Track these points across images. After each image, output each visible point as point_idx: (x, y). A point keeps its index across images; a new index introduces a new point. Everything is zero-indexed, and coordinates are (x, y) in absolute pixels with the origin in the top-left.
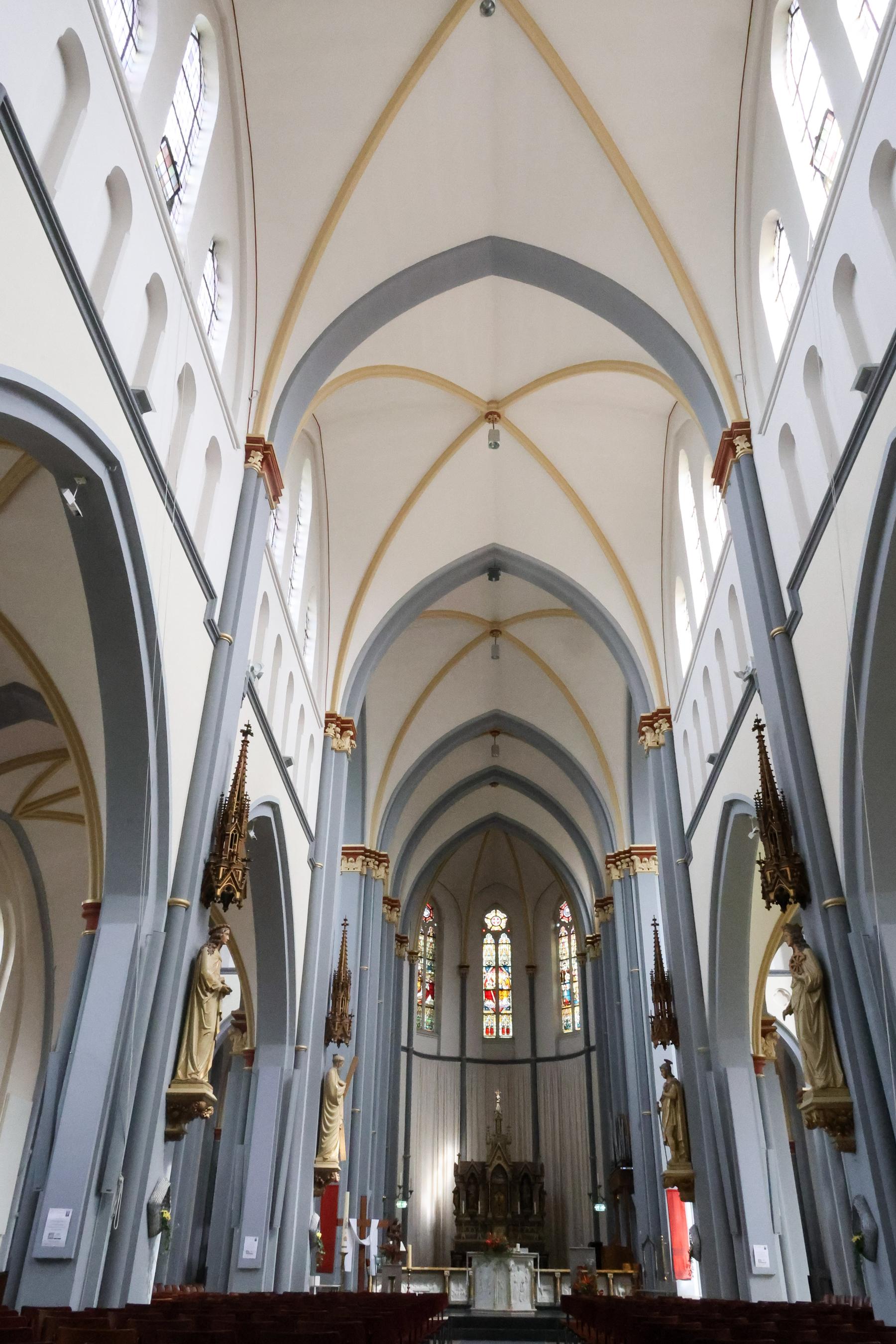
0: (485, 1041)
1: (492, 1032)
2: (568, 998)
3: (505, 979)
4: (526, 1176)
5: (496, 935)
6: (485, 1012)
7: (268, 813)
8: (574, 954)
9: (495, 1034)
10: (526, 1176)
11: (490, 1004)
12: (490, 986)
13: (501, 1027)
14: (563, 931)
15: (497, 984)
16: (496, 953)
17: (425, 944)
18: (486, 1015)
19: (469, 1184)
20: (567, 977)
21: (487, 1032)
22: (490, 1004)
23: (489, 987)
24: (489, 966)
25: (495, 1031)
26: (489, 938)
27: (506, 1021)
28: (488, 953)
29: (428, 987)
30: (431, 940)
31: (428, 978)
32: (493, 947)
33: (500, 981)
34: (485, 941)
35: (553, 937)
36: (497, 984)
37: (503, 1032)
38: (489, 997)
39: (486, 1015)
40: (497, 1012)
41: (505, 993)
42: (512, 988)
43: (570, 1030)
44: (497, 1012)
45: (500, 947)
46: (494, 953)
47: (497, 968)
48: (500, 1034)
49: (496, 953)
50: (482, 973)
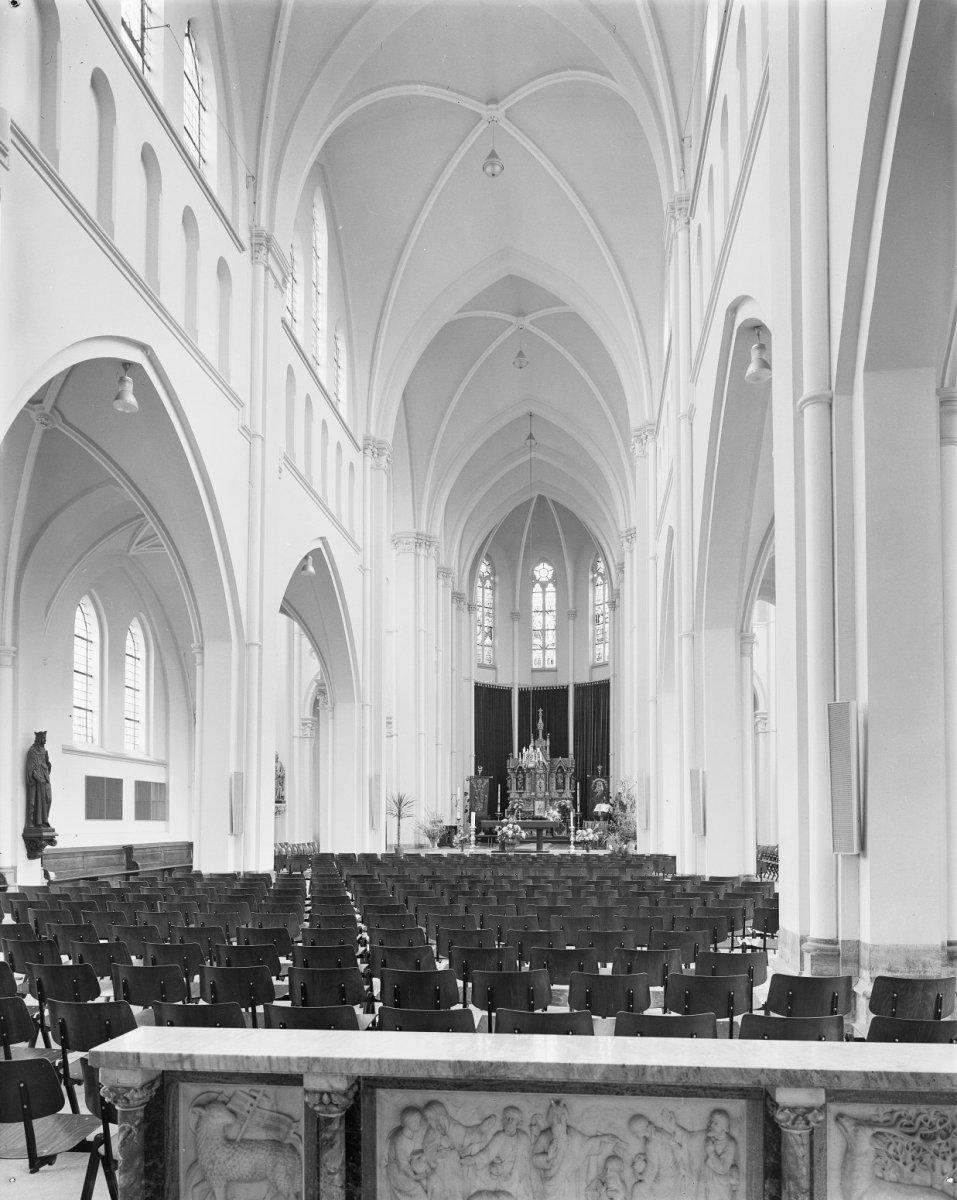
0: (533, 671)
1: (539, 663)
2: (601, 636)
3: (551, 621)
4: (560, 767)
5: (544, 585)
7: (319, 545)
8: (606, 600)
10: (560, 767)
11: (537, 641)
14: (599, 580)
15: (544, 625)
16: (544, 600)
17: (484, 596)
19: (518, 773)
20: (601, 619)
26: (537, 588)
27: (551, 654)
28: (537, 600)
29: (486, 630)
30: (488, 591)
31: (487, 623)
32: (541, 595)
33: (547, 623)
35: (591, 585)
36: (544, 625)
41: (550, 632)
42: (556, 629)
43: (601, 661)
44: (544, 648)
45: (547, 595)
46: (542, 600)
47: (544, 612)
49: (544, 600)
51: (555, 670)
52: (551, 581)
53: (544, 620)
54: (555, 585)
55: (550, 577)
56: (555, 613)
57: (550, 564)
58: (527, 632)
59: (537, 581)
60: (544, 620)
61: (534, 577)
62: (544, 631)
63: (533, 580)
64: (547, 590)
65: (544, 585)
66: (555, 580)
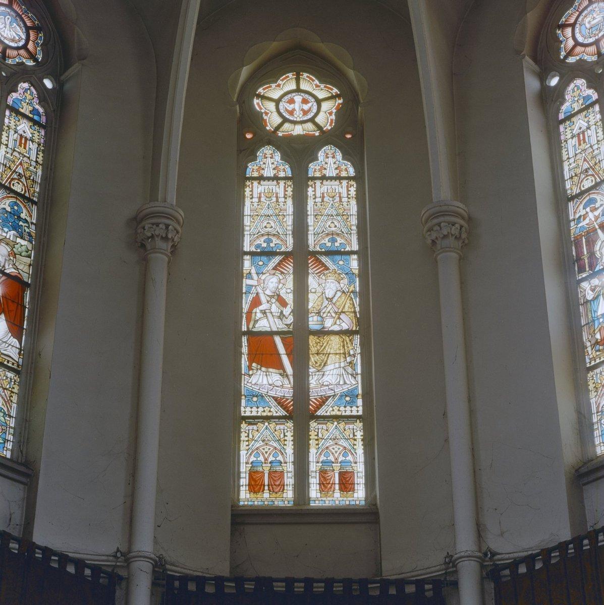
3: (333, 294)
11: (266, 383)
12: (269, 319)
15: (301, 310)
22: (266, 383)
23: (263, 325)
24: (270, 254)
26: (269, 161)
28: (264, 205)
32: (282, 190)
33: (313, 301)
34: (252, 169)
36: (301, 310)
42: (364, 328)
45: (315, 192)
47: (301, 258)
50: (239, 275)
52: (326, 138)
53: (301, 291)
54: (351, 152)
55: (327, 116)
56: (354, 263)
57: (327, 72)
60: (301, 291)
61: (253, 120)
63: (249, 135)
64: (313, 169)
65: (299, 152)
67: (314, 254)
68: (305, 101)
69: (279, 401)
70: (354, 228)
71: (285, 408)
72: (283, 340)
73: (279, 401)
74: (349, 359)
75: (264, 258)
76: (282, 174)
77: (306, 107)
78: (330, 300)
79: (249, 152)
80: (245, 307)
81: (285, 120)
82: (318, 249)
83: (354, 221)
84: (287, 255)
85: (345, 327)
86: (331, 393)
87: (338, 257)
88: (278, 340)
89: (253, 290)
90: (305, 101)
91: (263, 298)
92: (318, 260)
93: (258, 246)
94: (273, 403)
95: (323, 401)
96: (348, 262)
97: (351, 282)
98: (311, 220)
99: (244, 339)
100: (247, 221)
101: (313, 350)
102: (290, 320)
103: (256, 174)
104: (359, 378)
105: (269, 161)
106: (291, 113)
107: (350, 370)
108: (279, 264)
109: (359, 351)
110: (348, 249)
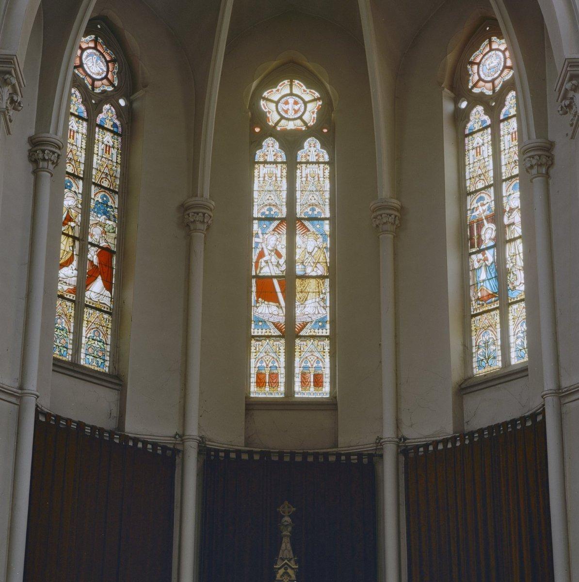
1: (274, 382)
3: (313, 249)
6: (255, 332)
9: (282, 388)
11: (267, 312)
13: (297, 371)
15: (291, 261)
18: (259, 338)
21: (260, 383)
22: (267, 312)
23: (266, 271)
24: (271, 219)
25: (282, 379)
26: (271, 149)
27: (315, 357)
28: (267, 185)
32: (280, 171)
33: (299, 254)
34: (259, 155)
36: (291, 261)
37: (304, 383)
38: (266, 293)
39: (259, 338)
40: (290, 333)
42: (333, 274)
45: (303, 172)
48: (297, 387)
50: (250, 235)
51: (329, 406)
55: (311, 116)
56: (327, 227)
57: (312, 81)
58: (237, 281)
59: (270, 132)
61: (259, 118)
62: (290, 280)
63: (256, 129)
64: (301, 155)
66: (326, 129)
67: (300, 219)
68: (296, 103)
69: (276, 325)
70: (327, 200)
71: (280, 330)
72: (279, 282)
73: (276, 325)
74: (321, 296)
75: (267, 222)
76: (279, 160)
77: (296, 107)
78: (310, 253)
79: (256, 142)
80: (254, 258)
81: (282, 118)
82: (303, 216)
83: (327, 195)
84: (282, 220)
85: (320, 273)
86: (309, 320)
87: (316, 222)
88: (275, 281)
89: (260, 246)
90: (296, 103)
91: (266, 252)
92: (303, 225)
93: (263, 214)
94: (272, 326)
95: (304, 325)
96: (322, 225)
97: (324, 241)
98: (298, 194)
99: (254, 281)
100: (256, 195)
101: (298, 289)
102: (284, 268)
103: (262, 160)
104: (328, 309)
105: (271, 149)
106: (286, 112)
107: (322, 304)
108: (277, 227)
109: (328, 290)
110: (323, 216)
